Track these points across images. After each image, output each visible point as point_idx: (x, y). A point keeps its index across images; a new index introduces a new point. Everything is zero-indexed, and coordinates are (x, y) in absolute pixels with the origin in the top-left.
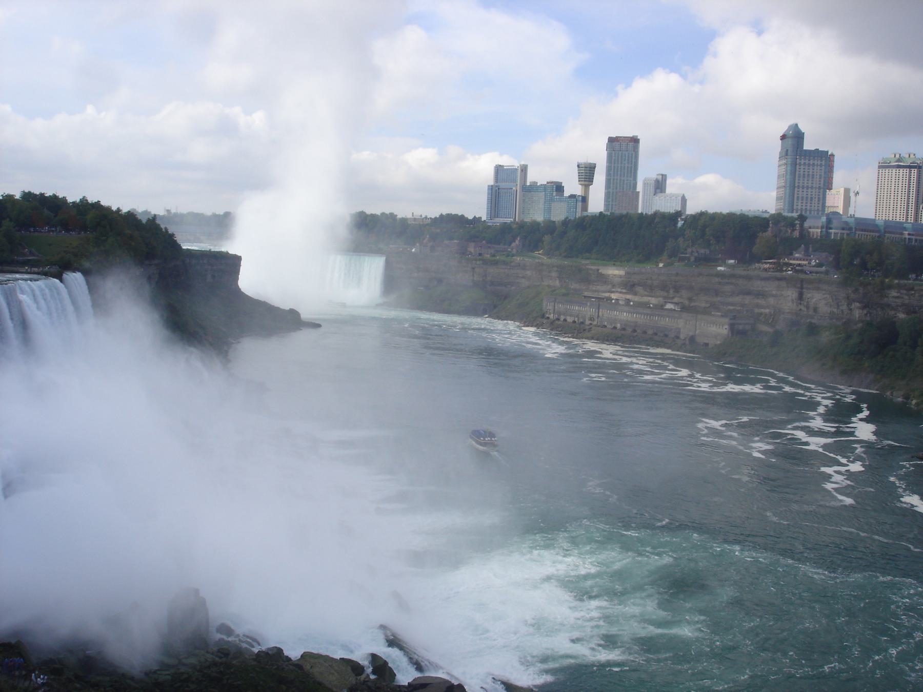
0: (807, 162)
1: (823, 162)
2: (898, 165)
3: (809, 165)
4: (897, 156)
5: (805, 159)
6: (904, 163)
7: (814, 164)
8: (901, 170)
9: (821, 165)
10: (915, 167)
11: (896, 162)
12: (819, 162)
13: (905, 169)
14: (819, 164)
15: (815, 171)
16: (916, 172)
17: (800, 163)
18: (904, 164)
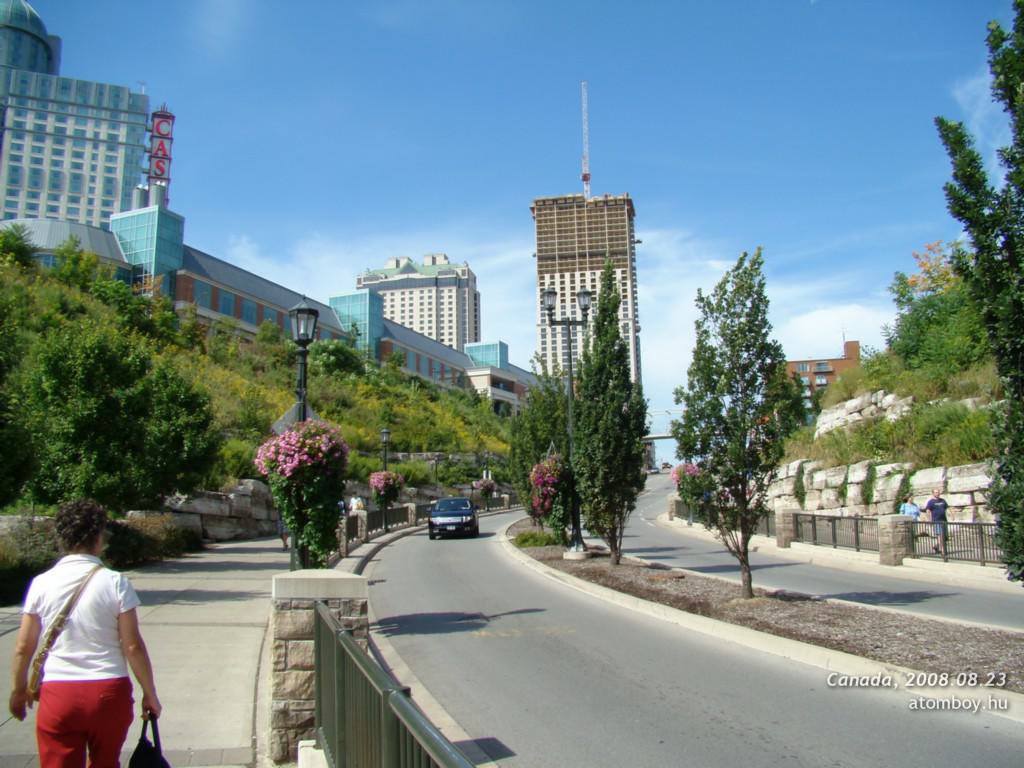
0: (51, 124)
1: (122, 133)
2: (408, 279)
3: (60, 136)
4: (403, 263)
5: (42, 116)
6: (422, 274)
7: (79, 138)
8: (417, 293)
9: (112, 143)
10: (448, 283)
11: (402, 272)
12: (104, 132)
13: (426, 290)
14: (103, 136)
15: (86, 161)
16: (454, 294)
17: (19, 131)
18: (424, 277)
